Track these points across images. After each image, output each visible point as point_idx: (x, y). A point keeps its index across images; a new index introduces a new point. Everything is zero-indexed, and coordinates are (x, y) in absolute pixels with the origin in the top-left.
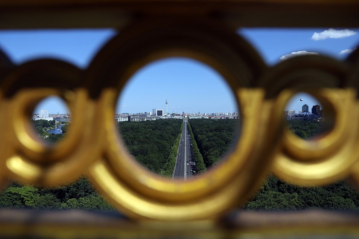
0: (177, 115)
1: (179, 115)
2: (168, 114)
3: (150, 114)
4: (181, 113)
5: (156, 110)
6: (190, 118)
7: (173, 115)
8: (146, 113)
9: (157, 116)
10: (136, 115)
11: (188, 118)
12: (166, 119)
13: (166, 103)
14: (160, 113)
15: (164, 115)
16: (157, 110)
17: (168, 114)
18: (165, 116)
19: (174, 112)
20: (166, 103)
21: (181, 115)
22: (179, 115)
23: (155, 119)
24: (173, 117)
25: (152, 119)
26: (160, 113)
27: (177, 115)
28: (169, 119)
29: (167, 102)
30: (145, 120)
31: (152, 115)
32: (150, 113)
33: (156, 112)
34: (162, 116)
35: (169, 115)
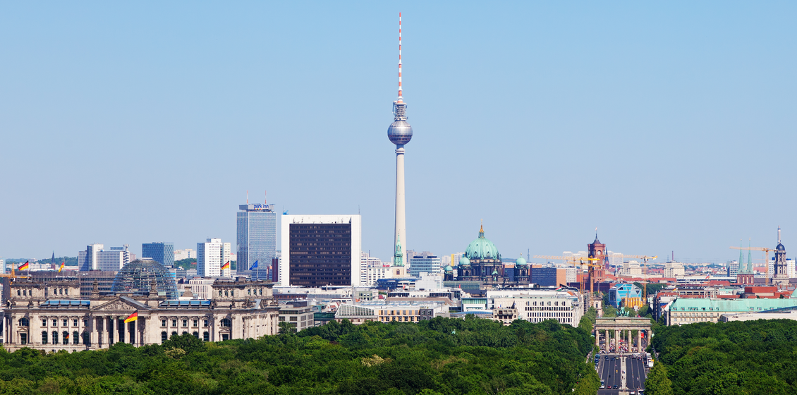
0: (516, 276)
1: (544, 278)
2: (421, 263)
3: (212, 268)
4: (570, 261)
5: (273, 228)
6: (683, 311)
7: (477, 272)
8: (155, 251)
9: (284, 284)
10: (40, 280)
11: (654, 313)
12: (392, 331)
13: (399, 140)
14: (322, 253)
15: (375, 274)
16: (285, 222)
17: (421, 263)
18: (383, 285)
19: (486, 249)
20: (399, 140)
21: (572, 278)
22: (544, 278)
23: (260, 328)
24: (480, 295)
25: (227, 323)
26: (322, 253)
27: (516, 276)
28: (430, 323)
29: (402, 129)
30: (153, 333)
31: (228, 272)
32: (211, 254)
33: (273, 243)
34: (342, 291)
35: (431, 282)
